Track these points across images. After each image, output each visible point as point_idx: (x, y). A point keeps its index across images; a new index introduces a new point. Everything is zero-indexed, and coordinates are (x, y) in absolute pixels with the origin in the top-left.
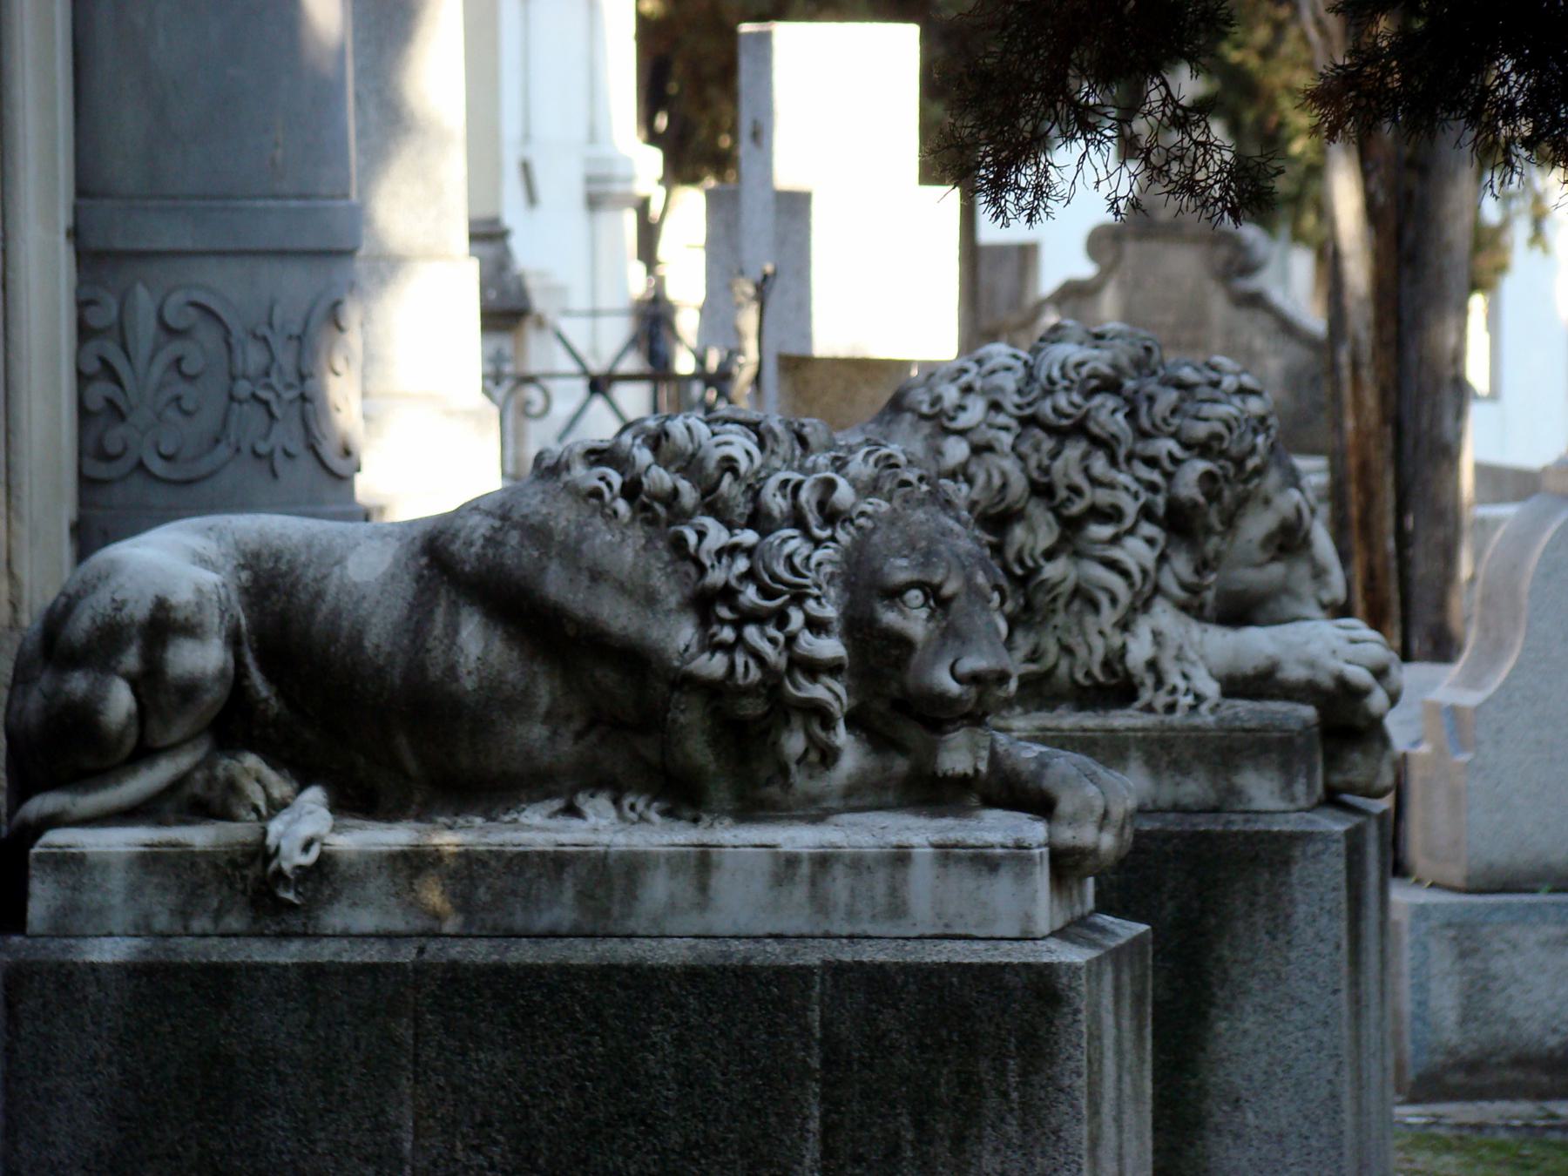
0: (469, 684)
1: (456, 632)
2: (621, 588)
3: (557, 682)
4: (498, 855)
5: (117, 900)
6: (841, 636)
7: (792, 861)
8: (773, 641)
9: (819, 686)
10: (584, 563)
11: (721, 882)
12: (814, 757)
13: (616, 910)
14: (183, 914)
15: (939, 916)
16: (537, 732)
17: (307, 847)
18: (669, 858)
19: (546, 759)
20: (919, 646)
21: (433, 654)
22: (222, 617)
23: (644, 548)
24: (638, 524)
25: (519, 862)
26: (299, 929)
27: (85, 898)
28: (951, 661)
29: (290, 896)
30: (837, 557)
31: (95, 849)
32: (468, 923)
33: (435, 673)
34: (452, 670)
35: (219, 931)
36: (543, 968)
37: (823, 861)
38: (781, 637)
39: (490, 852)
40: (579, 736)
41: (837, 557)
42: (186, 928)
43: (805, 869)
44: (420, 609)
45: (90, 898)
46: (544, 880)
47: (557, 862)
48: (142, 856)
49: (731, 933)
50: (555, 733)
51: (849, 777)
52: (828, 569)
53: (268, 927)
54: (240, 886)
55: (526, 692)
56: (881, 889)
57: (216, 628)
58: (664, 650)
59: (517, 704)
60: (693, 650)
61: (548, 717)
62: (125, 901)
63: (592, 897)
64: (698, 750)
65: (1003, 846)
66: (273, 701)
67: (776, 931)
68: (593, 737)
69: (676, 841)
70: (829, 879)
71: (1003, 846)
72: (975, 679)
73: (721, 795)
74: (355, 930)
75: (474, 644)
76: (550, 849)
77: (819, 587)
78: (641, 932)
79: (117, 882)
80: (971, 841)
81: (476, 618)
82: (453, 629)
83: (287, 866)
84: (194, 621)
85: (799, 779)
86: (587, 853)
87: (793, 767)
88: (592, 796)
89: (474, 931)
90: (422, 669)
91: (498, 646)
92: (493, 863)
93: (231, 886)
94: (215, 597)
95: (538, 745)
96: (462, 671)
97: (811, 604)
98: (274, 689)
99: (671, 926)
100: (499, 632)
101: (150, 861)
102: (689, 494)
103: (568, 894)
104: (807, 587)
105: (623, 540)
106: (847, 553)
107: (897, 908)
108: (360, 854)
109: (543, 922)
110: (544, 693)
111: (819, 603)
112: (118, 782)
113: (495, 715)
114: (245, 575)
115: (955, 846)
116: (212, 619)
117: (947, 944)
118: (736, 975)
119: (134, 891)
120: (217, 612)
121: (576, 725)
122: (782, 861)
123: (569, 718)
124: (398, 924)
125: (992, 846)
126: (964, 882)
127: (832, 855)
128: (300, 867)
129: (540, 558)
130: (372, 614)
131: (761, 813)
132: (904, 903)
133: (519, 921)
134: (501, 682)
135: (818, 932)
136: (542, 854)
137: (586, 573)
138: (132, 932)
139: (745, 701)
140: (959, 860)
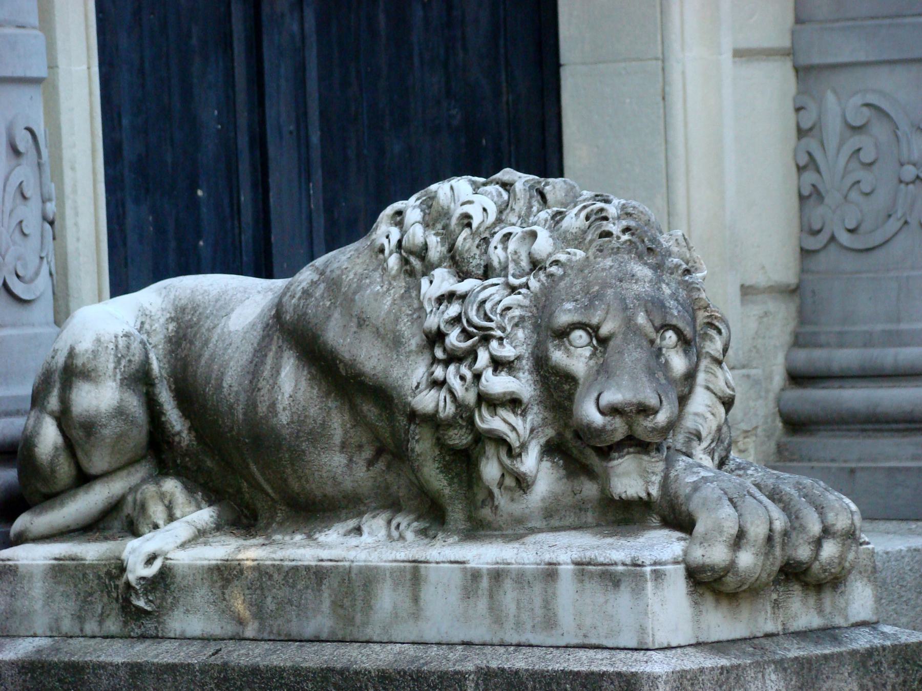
0: (284, 418)
1: (278, 372)
2: (377, 333)
3: (347, 417)
4: (279, 568)
5: (38, 606)
6: (531, 373)
7: (475, 575)
8: (463, 378)
9: (497, 418)
10: (356, 311)
11: (428, 594)
12: (509, 482)
13: (359, 618)
14: (80, 618)
15: (579, 627)
16: (335, 461)
17: (151, 560)
18: (392, 571)
19: (348, 484)
20: (581, 381)
21: (262, 392)
22: (118, 362)
23: (402, 297)
24: (402, 276)
25: (293, 574)
26: (152, 632)
27: (19, 603)
28: (596, 395)
29: (141, 603)
30: (527, 302)
31: (25, 562)
32: (261, 630)
33: (262, 409)
34: (273, 405)
35: (103, 633)
36: (283, 670)
37: (497, 575)
38: (469, 375)
39: (274, 566)
40: (370, 463)
41: (527, 302)
42: (82, 630)
43: (485, 583)
44: (260, 352)
45: (21, 604)
46: (309, 591)
47: (318, 575)
48: (53, 567)
49: (437, 640)
50: (351, 460)
51: (543, 500)
52: (517, 312)
53: (133, 630)
54: (114, 595)
55: (323, 425)
56: (538, 602)
57: (110, 372)
58: (401, 386)
59: (318, 436)
60: (422, 387)
61: (344, 446)
62: (43, 607)
63: (342, 606)
64: (434, 477)
65: (624, 564)
66: (185, 434)
67: (467, 639)
68: (381, 465)
69: (398, 558)
70: (501, 593)
71: (624, 564)
72: (614, 411)
73: (456, 516)
74: (189, 634)
75: (290, 385)
76: (313, 563)
77: (503, 329)
78: (375, 638)
79: (38, 589)
80: (601, 559)
81: (292, 360)
82: (276, 371)
83: (131, 577)
84: (89, 366)
85: (502, 500)
86: (336, 567)
87: (496, 491)
88: (374, 517)
89: (266, 636)
90: (255, 406)
91: (303, 384)
92: (276, 576)
93: (109, 593)
94: (111, 346)
95: (339, 471)
96: (280, 407)
97: (494, 344)
98: (188, 424)
99: (397, 635)
100: (305, 373)
101: (60, 571)
102: (436, 249)
103: (326, 605)
104: (491, 329)
105: (388, 290)
106: (536, 297)
107: (550, 622)
108: (190, 567)
109: (310, 630)
110: (339, 425)
111: (501, 344)
112: (62, 505)
113: (304, 446)
114: (172, 326)
115: (589, 564)
116: (107, 363)
117: (581, 653)
118: (412, 679)
119: (49, 597)
120: (112, 358)
121: (368, 453)
122: (469, 574)
123: (360, 447)
124: (215, 629)
125: (616, 564)
126: (595, 594)
127: (503, 570)
128: (143, 578)
129: (329, 308)
130: (231, 358)
131: (483, 533)
132: (555, 615)
133: (294, 628)
134: (306, 416)
135: (496, 641)
136: (308, 568)
137: (355, 320)
138: (49, 634)
139: (452, 432)
140: (591, 575)
